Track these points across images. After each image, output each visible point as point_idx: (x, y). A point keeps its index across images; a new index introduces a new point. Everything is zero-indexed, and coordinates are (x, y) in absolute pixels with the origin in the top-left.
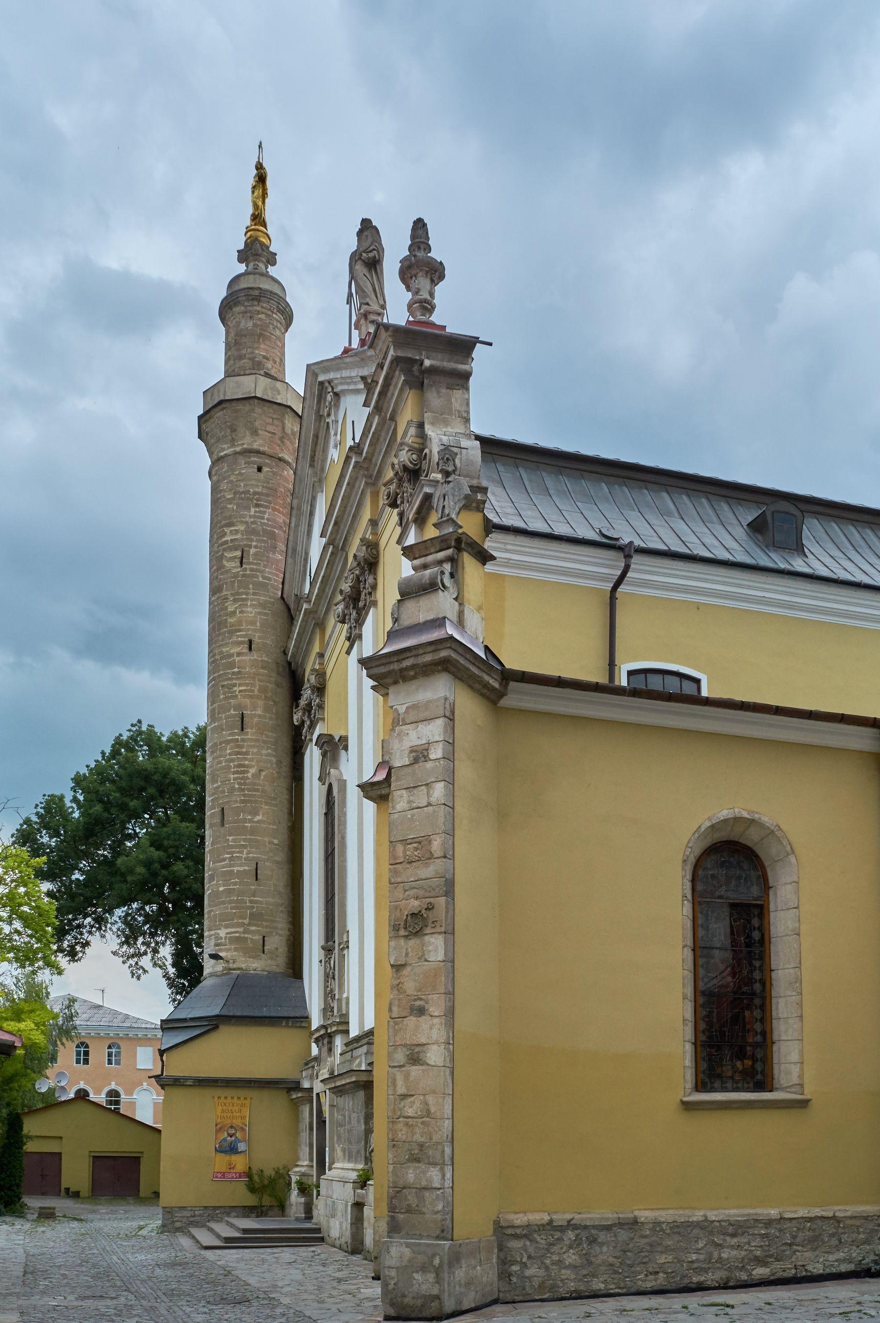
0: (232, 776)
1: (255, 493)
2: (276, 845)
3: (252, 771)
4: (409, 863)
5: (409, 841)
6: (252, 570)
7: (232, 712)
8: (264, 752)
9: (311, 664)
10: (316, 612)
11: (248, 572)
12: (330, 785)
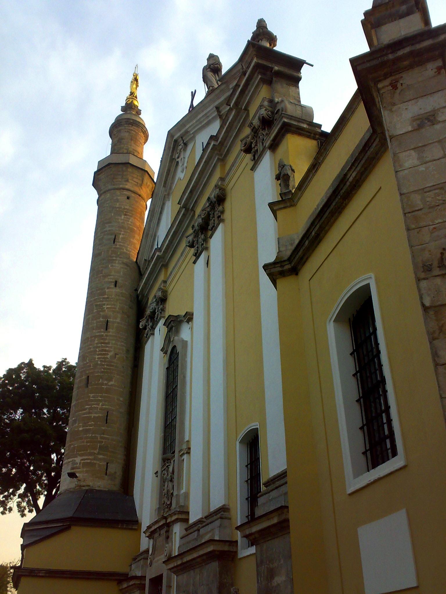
0: (97, 357)
1: (124, 209)
2: (121, 401)
3: (111, 354)
4: (430, 208)
5: (425, 190)
6: (120, 245)
7: (101, 319)
8: (119, 343)
9: (155, 293)
10: (163, 258)
11: (118, 246)
12: (174, 347)
